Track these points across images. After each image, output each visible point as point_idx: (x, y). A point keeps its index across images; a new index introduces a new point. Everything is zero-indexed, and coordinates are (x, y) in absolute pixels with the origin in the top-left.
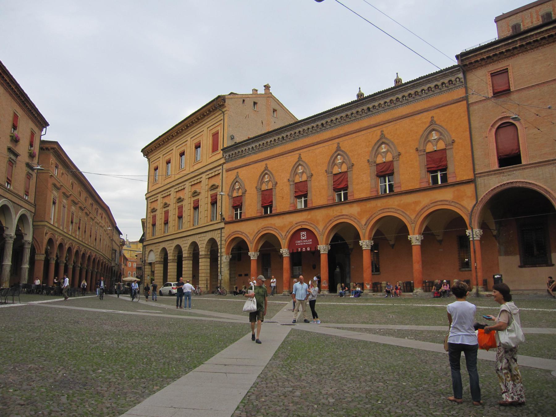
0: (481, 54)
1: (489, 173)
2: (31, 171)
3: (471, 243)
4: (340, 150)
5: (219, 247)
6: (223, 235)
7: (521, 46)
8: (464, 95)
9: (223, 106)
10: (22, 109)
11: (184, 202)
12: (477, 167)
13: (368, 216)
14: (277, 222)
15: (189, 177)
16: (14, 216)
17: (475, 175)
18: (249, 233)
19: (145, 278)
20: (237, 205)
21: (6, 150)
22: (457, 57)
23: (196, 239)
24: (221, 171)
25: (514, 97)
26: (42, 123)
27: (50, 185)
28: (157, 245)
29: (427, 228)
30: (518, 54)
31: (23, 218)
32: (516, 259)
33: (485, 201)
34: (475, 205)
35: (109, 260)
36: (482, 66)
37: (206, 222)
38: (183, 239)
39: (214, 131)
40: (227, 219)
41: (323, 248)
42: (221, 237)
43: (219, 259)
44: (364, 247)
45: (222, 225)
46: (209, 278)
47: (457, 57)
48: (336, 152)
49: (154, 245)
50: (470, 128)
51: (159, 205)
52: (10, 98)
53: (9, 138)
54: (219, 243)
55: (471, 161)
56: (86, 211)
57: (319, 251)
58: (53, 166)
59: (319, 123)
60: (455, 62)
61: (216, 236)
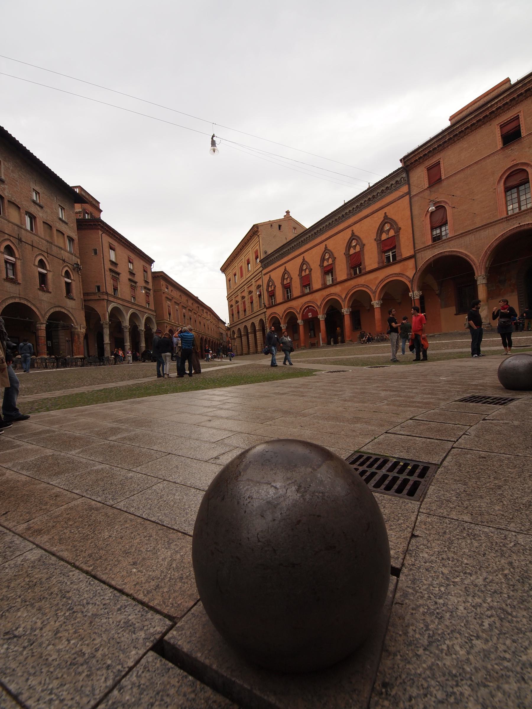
0: (419, 153)
2: (148, 291)
7: (450, 139)
9: (257, 231)
10: (133, 253)
12: (416, 246)
13: (346, 293)
14: (293, 304)
16: (141, 319)
17: (415, 251)
21: (128, 280)
22: (401, 160)
23: (253, 320)
25: (445, 183)
26: (150, 261)
27: (164, 298)
29: (386, 294)
30: (447, 146)
31: (148, 320)
32: (453, 310)
34: (415, 274)
35: (218, 339)
36: (420, 163)
40: (267, 306)
41: (321, 317)
45: (265, 310)
47: (401, 160)
48: (324, 251)
51: (233, 303)
52: (123, 248)
53: (128, 273)
55: (412, 242)
56: (194, 311)
58: (164, 286)
59: (313, 233)
60: (400, 165)
61: (262, 317)
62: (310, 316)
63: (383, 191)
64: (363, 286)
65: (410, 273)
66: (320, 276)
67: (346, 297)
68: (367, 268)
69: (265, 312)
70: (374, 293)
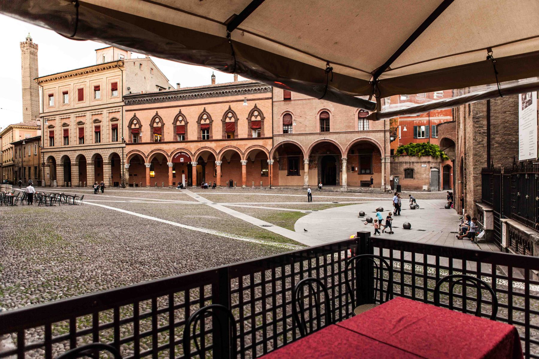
1: (279, 135)
3: (269, 166)
4: (206, 112)
5: (121, 159)
6: (124, 151)
8: (271, 97)
11: (85, 125)
12: (274, 132)
13: (220, 149)
15: (90, 108)
18: (145, 152)
19: (45, 176)
20: (135, 133)
24: (121, 110)
25: (292, 102)
28: (58, 153)
32: (286, 172)
33: (276, 148)
37: (108, 141)
38: (86, 151)
39: (113, 81)
40: (128, 142)
42: (123, 152)
43: (122, 166)
44: (218, 164)
45: (124, 145)
46: (111, 177)
48: (203, 112)
49: (54, 153)
50: (273, 113)
54: (121, 156)
57: (192, 165)
59: (194, 94)
61: (119, 152)
62: (181, 161)
63: (255, 90)
64: (235, 147)
65: (269, 148)
66: (197, 131)
67: (219, 153)
68: (239, 136)
69: (123, 148)
70: (244, 154)
